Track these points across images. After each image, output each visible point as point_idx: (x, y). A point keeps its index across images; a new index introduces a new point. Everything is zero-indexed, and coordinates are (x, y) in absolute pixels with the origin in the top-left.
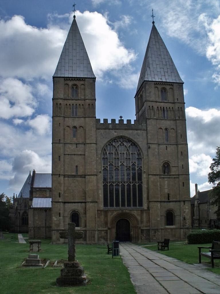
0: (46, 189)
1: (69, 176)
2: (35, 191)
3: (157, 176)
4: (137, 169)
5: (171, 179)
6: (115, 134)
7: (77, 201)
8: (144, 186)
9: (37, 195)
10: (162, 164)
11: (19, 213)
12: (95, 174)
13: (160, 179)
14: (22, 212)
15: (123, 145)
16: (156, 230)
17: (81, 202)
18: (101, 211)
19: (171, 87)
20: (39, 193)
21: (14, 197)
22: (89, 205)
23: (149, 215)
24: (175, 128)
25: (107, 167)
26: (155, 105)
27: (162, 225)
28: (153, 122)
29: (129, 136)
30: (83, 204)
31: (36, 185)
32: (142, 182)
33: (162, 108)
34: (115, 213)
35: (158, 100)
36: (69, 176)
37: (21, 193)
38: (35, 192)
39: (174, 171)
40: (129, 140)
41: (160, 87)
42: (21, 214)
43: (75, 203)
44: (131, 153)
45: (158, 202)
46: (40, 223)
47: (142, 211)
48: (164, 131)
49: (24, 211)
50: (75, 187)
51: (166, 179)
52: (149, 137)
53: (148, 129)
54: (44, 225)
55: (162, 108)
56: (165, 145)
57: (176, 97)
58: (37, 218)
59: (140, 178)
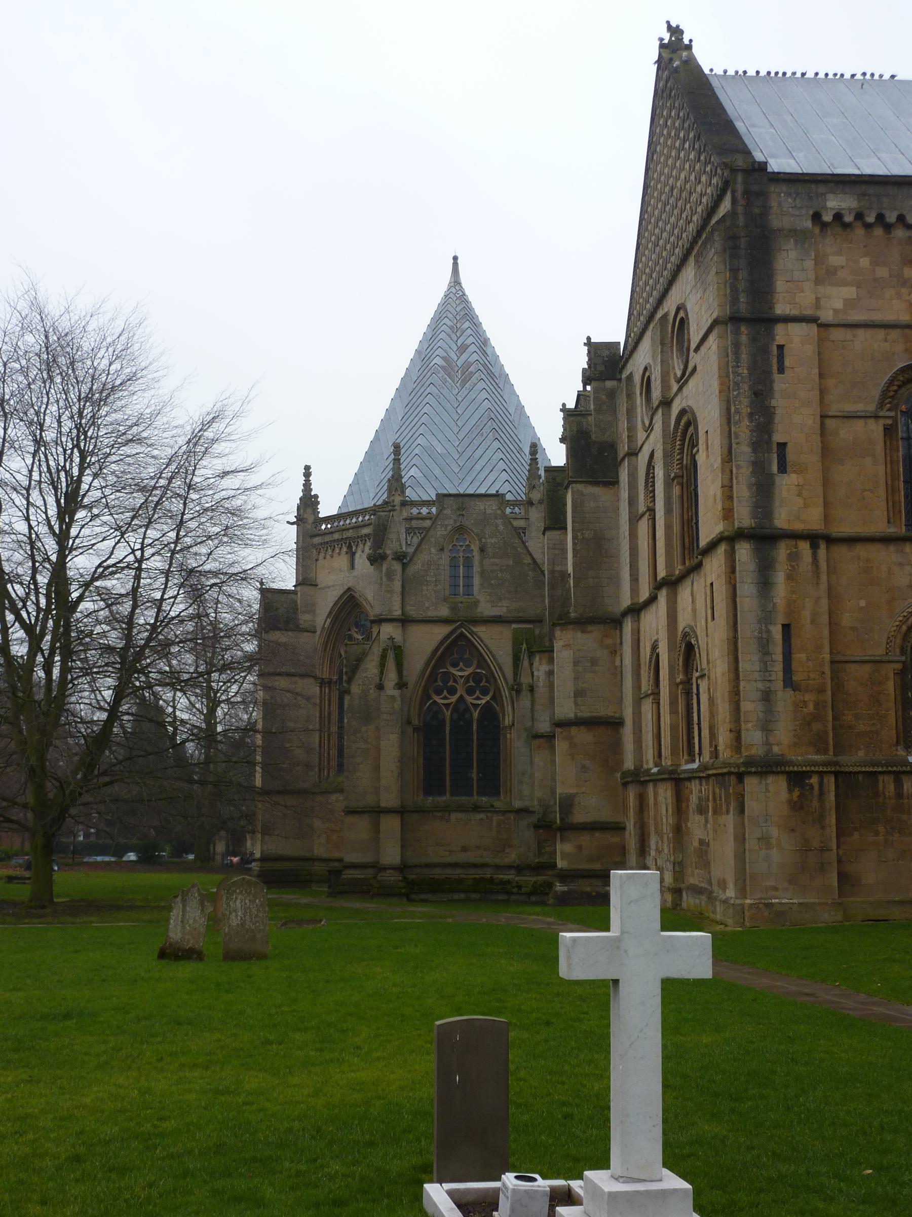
2: (809, 224)
9: (826, 290)
20: (865, 262)
21: (309, 502)
38: (799, 236)
42: (416, 664)
49: (441, 631)
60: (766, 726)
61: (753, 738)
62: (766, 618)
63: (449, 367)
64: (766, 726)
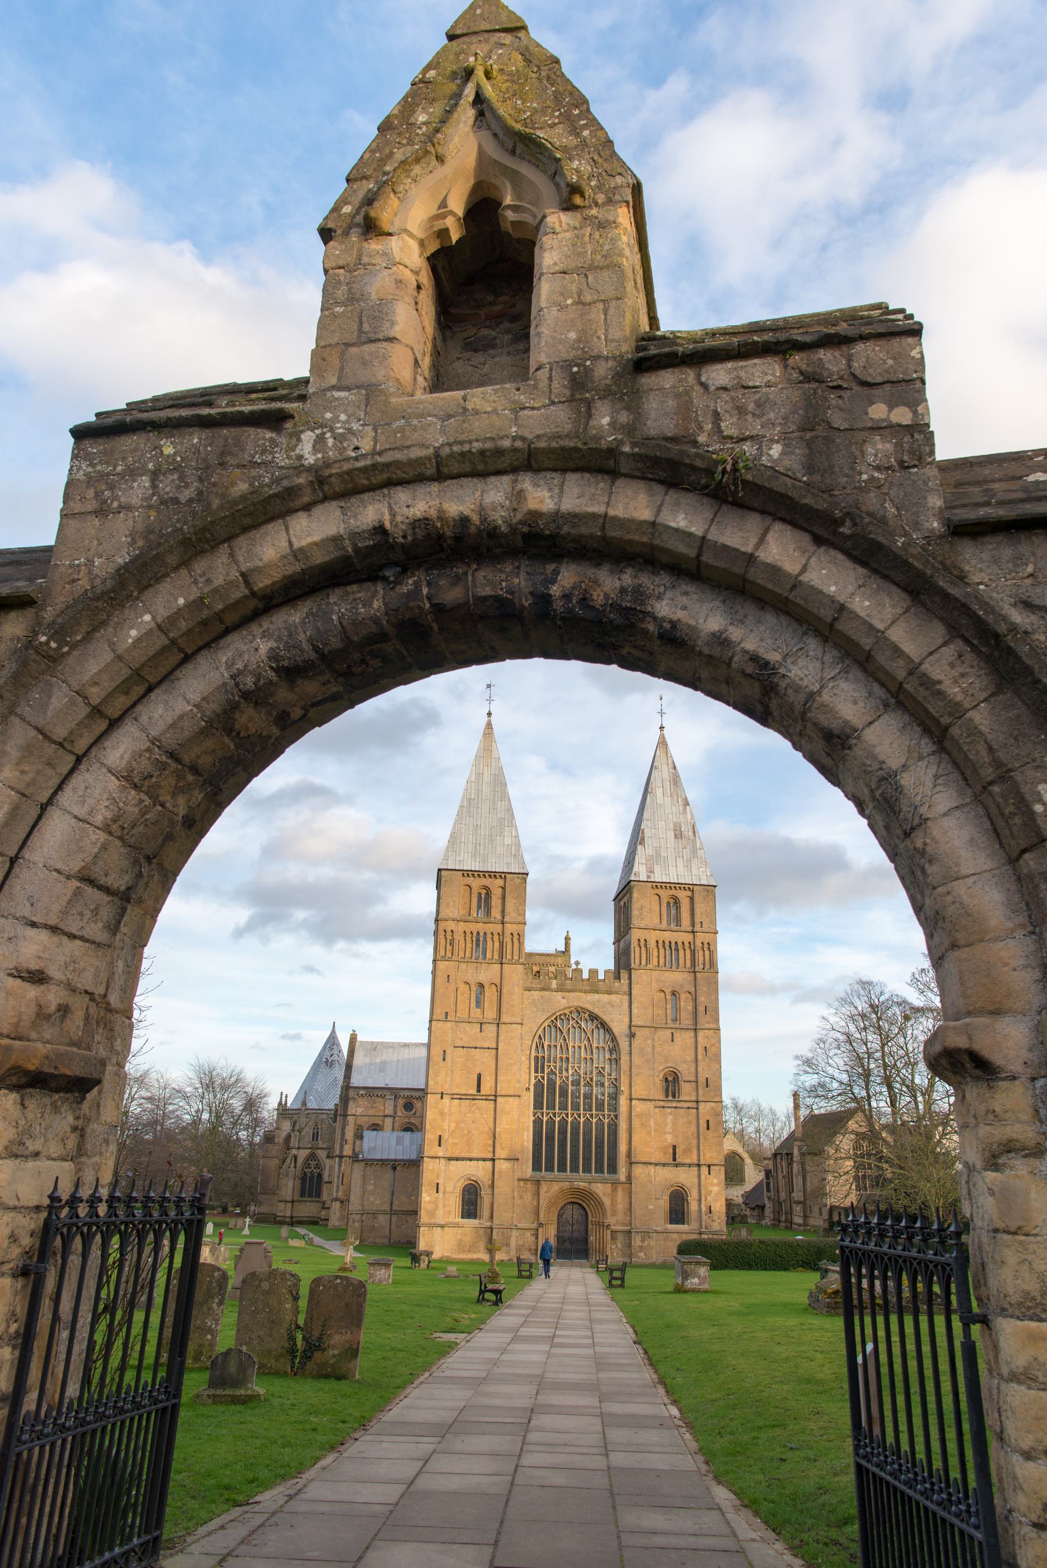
0: (385, 1092)
1: (461, 1097)
3: (649, 1103)
4: (606, 1084)
5: (681, 1111)
6: (561, 1001)
7: (475, 1155)
8: (623, 1126)
10: (661, 1075)
11: (296, 1157)
12: (517, 1093)
13: (657, 1110)
14: (303, 1154)
15: (580, 1027)
16: (646, 1234)
17: (484, 1160)
18: (525, 1180)
19: (689, 894)
22: (502, 1166)
23: (630, 1198)
24: (692, 990)
25: (543, 1078)
26: (652, 937)
27: (659, 1221)
28: (644, 977)
29: (591, 1009)
30: (489, 1164)
31: (356, 1080)
32: (616, 1116)
33: (667, 943)
34: (556, 1187)
35: (659, 927)
36: (461, 1097)
37: (305, 1091)
38: (354, 1099)
39: (687, 1091)
40: (593, 1017)
41: (665, 894)
42: (300, 1161)
43: (471, 1160)
44: (595, 1045)
45: (650, 1164)
46: (377, 1202)
47: (615, 1184)
48: (669, 997)
49: (309, 1151)
50: (473, 1122)
51: (669, 1110)
52: (635, 1011)
53: (634, 992)
54: (386, 1207)
55: (667, 943)
56: (670, 1031)
57: (697, 920)
58: (370, 1188)
59: (614, 1108)
60: (337, 1192)
61: (335, 1195)
62: (339, 1171)
63: (327, 1062)
64: (337, 1192)
